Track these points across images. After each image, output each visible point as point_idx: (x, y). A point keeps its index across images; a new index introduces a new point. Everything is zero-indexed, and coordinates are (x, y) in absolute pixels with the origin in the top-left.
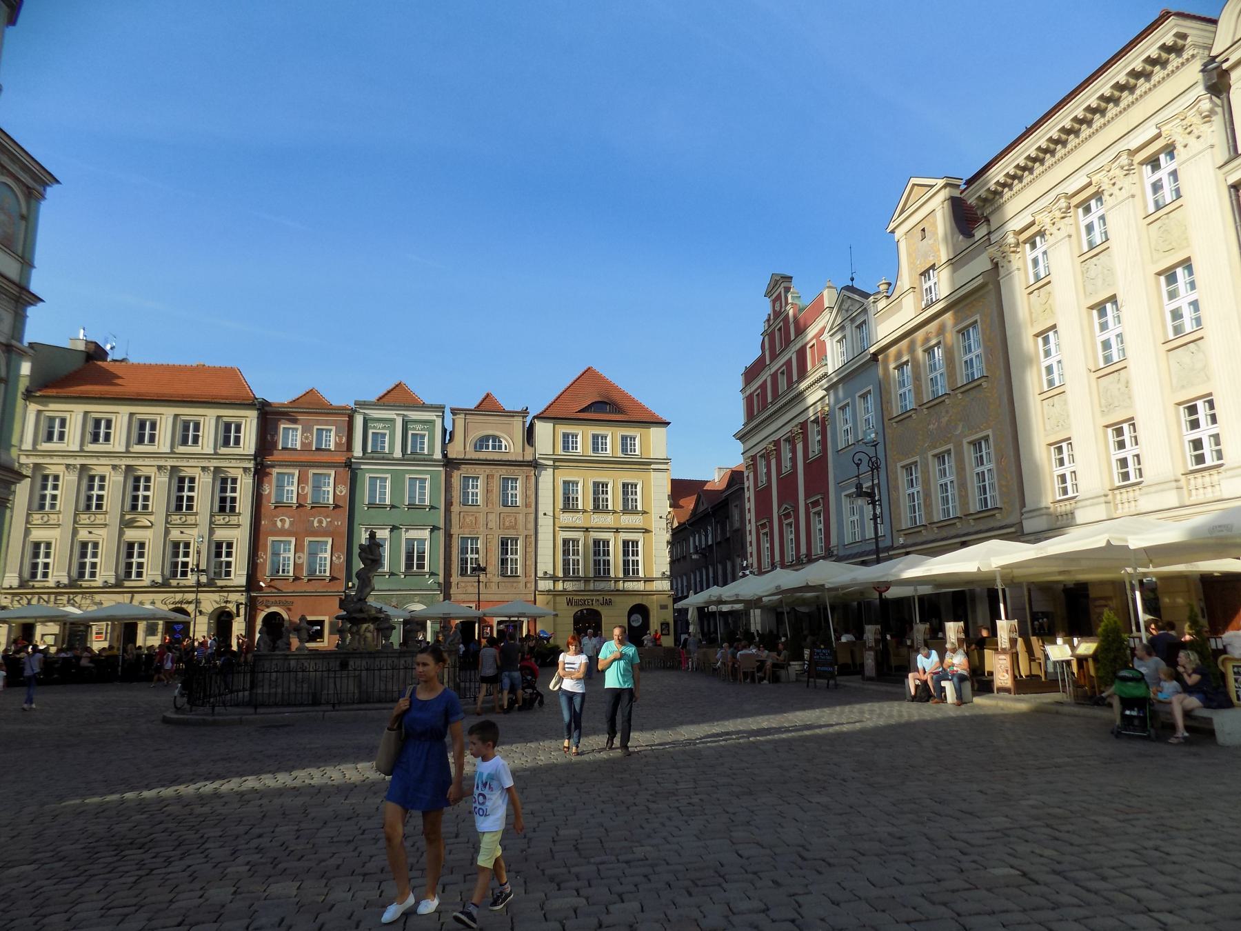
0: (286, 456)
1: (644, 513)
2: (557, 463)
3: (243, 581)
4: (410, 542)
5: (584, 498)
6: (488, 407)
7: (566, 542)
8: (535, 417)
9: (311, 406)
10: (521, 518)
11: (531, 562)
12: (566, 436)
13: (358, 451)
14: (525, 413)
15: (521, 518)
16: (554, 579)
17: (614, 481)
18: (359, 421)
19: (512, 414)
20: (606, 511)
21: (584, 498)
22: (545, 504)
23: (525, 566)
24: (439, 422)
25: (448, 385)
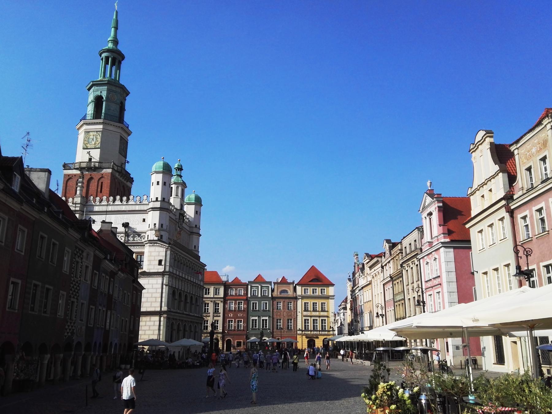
0: (231, 297)
1: (327, 311)
2: (303, 298)
3: (221, 331)
4: (263, 320)
5: (310, 308)
6: (284, 281)
7: (305, 320)
8: (296, 285)
9: (237, 283)
10: (293, 313)
11: (295, 326)
12: (305, 289)
13: (249, 296)
14: (293, 283)
15: (293, 313)
16: (302, 331)
17: (319, 302)
18: (249, 287)
19: (290, 284)
20: (316, 311)
21: (310, 308)
22: (299, 309)
23: (294, 327)
24: (270, 287)
25: (272, 275)
